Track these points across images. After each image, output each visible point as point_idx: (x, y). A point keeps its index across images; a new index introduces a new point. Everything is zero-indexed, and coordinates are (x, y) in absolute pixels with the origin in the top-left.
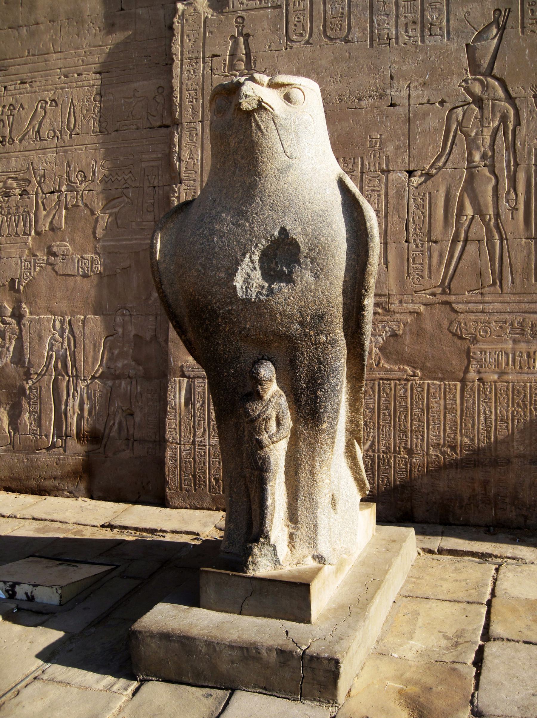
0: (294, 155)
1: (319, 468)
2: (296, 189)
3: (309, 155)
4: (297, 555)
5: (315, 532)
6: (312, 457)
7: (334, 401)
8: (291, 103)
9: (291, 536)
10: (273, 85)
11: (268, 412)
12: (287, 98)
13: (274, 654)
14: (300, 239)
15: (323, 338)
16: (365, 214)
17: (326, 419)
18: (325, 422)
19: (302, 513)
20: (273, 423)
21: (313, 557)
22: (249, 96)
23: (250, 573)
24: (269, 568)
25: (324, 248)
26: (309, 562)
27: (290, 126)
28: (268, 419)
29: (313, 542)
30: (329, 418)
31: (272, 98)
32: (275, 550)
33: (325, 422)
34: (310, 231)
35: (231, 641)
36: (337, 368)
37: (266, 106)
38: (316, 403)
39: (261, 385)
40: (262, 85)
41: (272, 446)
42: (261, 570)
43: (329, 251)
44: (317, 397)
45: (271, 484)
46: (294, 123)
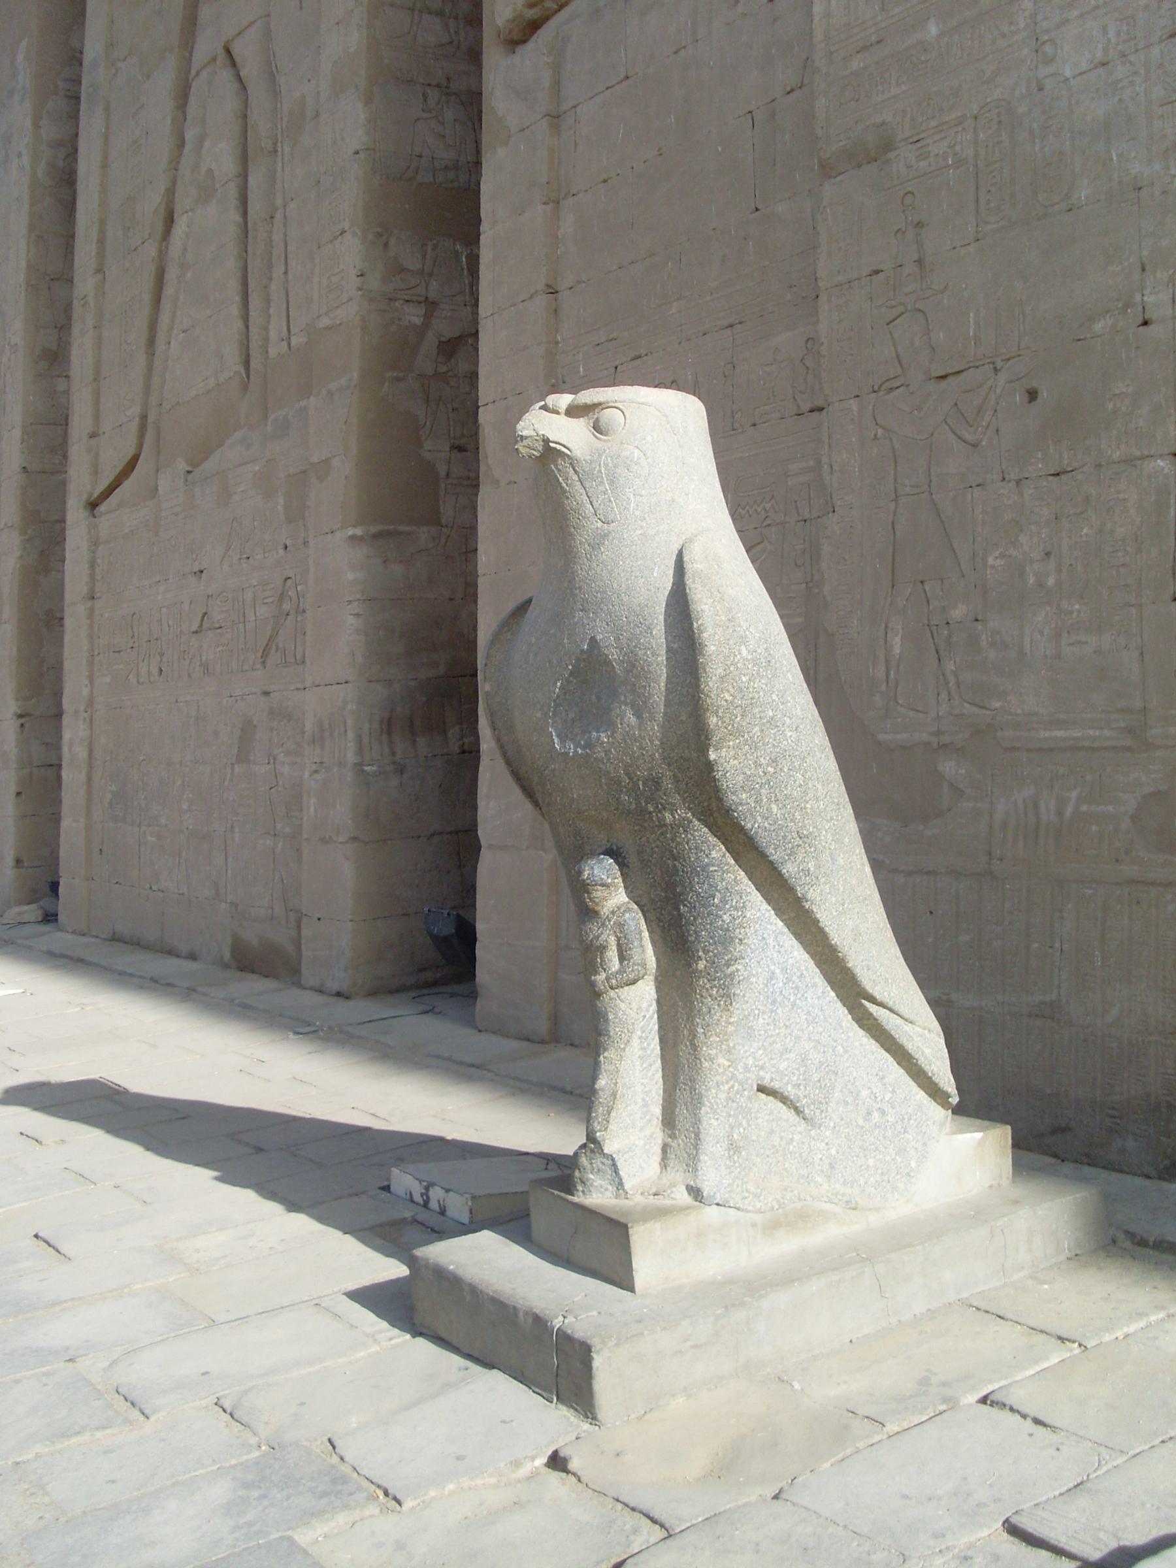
0: (611, 517)
1: (702, 1037)
2: (610, 572)
3: (638, 513)
4: (664, 1181)
5: (696, 1147)
6: (690, 1018)
7: (711, 924)
8: (601, 434)
9: (665, 1148)
10: (573, 411)
11: (603, 937)
12: (598, 428)
13: (530, 1321)
14: (614, 655)
15: (668, 817)
16: (693, 607)
17: (701, 953)
18: (700, 958)
19: (682, 1111)
20: (612, 954)
21: (687, 1187)
22: (526, 438)
23: (577, 1199)
24: (609, 1194)
25: (643, 669)
26: (678, 1196)
27: (600, 471)
28: (603, 948)
29: (692, 1163)
30: (706, 952)
31: (569, 434)
32: (614, 1165)
33: (700, 958)
34: (624, 641)
35: (495, 1292)
36: (704, 868)
37: (558, 447)
38: (681, 927)
39: (588, 893)
40: (558, 413)
41: (612, 993)
42: (594, 1195)
43: (650, 672)
44: (680, 916)
45: (606, 1054)
46: (606, 465)
